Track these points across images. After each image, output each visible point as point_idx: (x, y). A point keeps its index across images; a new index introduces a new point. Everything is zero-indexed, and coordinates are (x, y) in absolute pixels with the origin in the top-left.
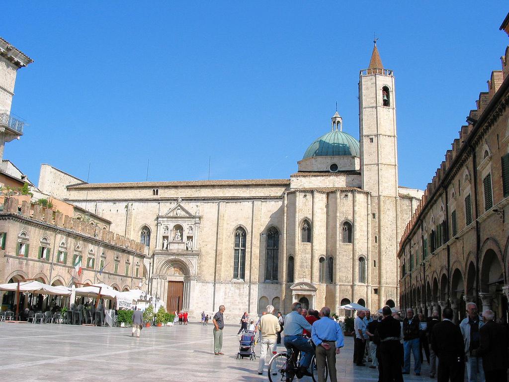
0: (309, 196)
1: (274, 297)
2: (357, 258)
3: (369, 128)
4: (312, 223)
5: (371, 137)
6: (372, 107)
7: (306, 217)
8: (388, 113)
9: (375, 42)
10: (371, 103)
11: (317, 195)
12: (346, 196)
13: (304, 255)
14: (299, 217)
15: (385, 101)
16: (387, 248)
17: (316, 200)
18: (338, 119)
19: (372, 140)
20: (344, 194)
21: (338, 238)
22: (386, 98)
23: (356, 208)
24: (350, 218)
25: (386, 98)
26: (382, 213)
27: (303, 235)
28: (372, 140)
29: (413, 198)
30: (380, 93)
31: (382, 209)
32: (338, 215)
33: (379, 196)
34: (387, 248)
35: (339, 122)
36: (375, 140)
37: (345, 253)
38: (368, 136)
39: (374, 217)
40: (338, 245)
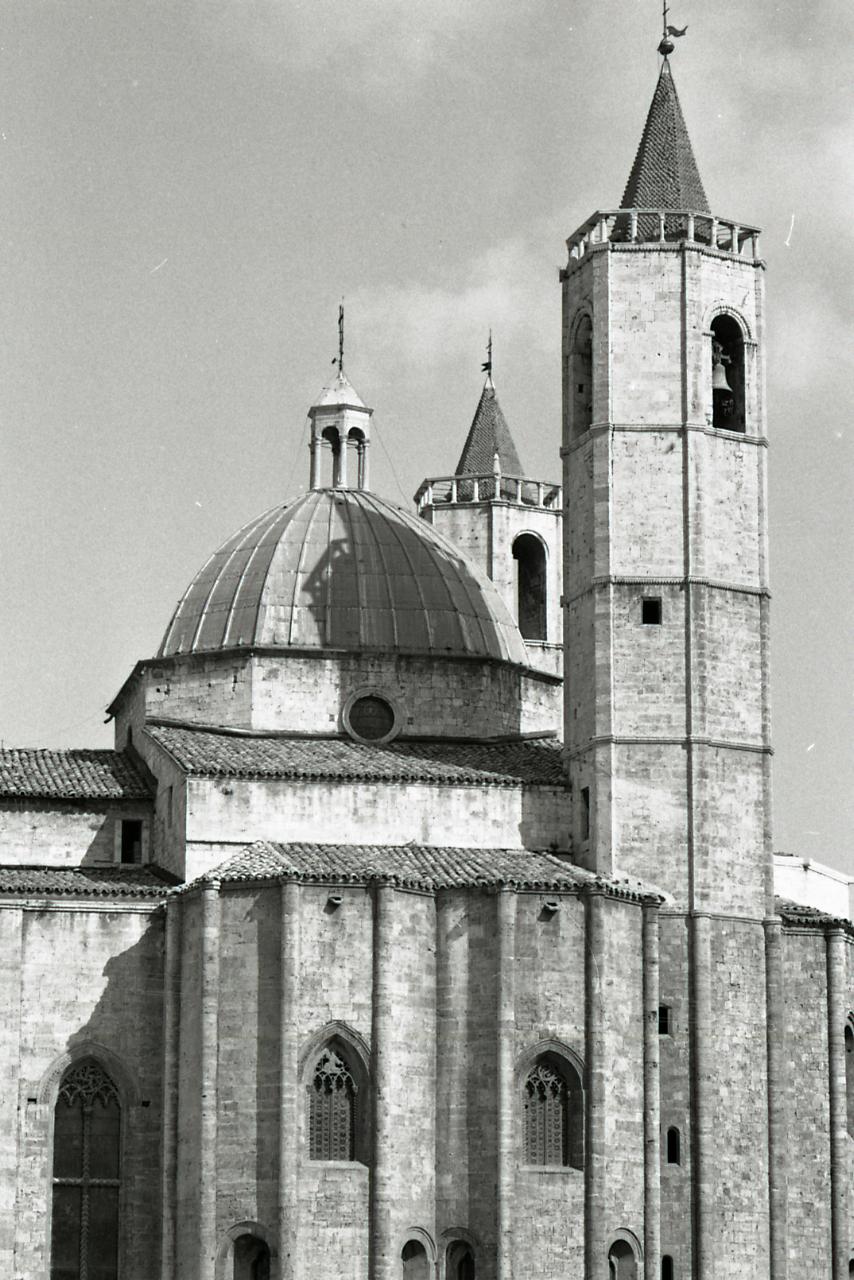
0: (355, 912)
2: (602, 1246)
3: (641, 541)
4: (375, 1053)
5: (648, 592)
6: (663, 429)
7: (340, 1024)
8: (733, 465)
9: (665, 49)
11: (402, 910)
12: (548, 914)
13: (330, 1232)
14: (302, 1024)
15: (718, 395)
16: (726, 1191)
17: (393, 931)
18: (352, 420)
19: (652, 613)
20: (537, 904)
21: (506, 1143)
22: (723, 384)
23: (600, 986)
24: (569, 1031)
25: (723, 384)
26: (705, 1006)
27: (317, 1121)
28: (652, 613)
29: (836, 924)
30: (703, 350)
31: (705, 982)
32: (508, 1014)
33: (691, 918)
34: (726, 1191)
35: (356, 434)
36: (673, 610)
37: (541, 1223)
38: (635, 586)
39: (664, 1028)
40: (506, 1179)
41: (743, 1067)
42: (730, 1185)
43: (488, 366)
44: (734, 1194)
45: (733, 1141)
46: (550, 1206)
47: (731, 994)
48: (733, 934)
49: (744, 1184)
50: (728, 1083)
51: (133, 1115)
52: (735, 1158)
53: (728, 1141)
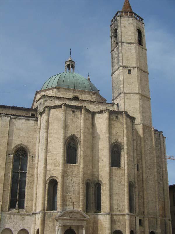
1: (20, 229)
3: (128, 60)
5: (130, 69)
10: (129, 40)
13: (71, 178)
19: (129, 71)
22: (139, 39)
28: (129, 71)
38: (127, 67)
41: (149, 154)
42: (148, 176)
43: (88, 75)
44: (149, 177)
45: (148, 167)
46: (117, 175)
47: (147, 140)
48: (146, 129)
49: (150, 176)
50: (147, 156)
51: (29, 158)
52: (149, 170)
53: (147, 167)
